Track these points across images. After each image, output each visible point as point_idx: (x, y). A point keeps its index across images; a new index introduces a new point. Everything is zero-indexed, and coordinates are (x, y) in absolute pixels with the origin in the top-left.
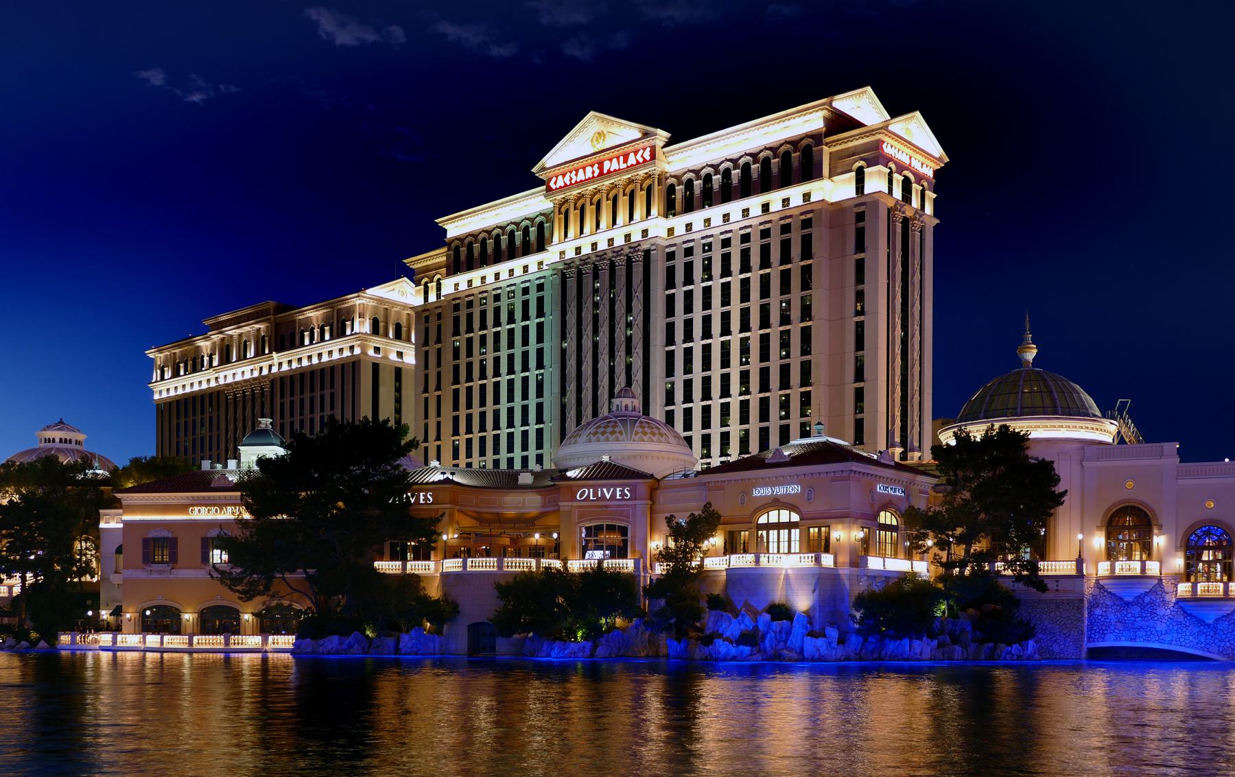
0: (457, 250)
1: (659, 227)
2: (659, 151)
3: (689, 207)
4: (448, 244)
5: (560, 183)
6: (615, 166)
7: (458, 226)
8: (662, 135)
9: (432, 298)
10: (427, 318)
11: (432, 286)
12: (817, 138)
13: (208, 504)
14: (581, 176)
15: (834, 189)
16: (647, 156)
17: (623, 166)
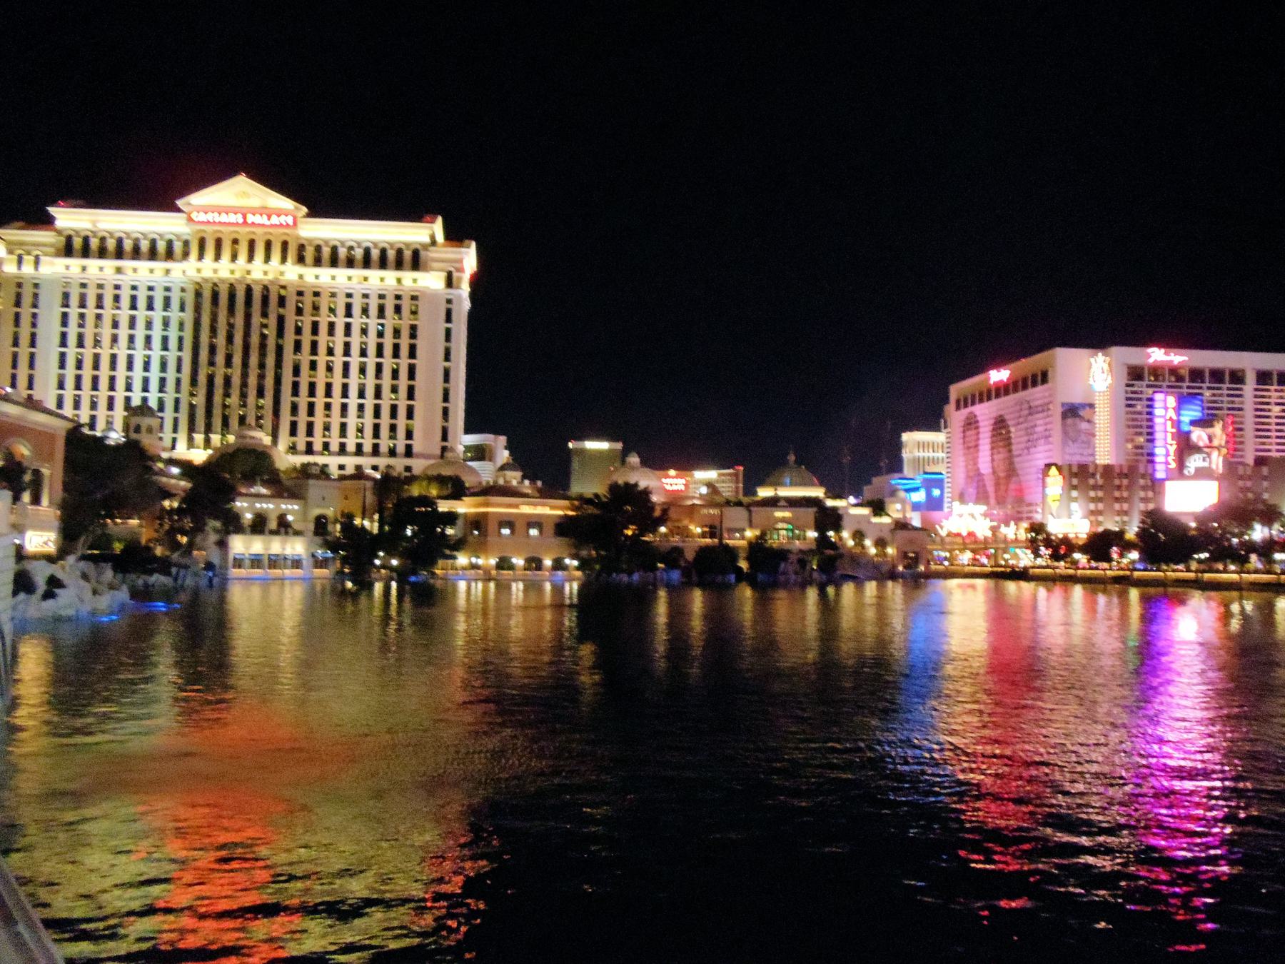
0: (69, 239)
1: (291, 273)
2: (300, 220)
3: (318, 262)
4: (59, 232)
5: (202, 217)
6: (257, 219)
7: (69, 218)
8: (305, 210)
9: (28, 269)
10: (19, 285)
11: (28, 259)
12: (425, 247)
13: (528, 504)
14: (224, 218)
15: (431, 281)
16: (290, 220)
17: (268, 223)
